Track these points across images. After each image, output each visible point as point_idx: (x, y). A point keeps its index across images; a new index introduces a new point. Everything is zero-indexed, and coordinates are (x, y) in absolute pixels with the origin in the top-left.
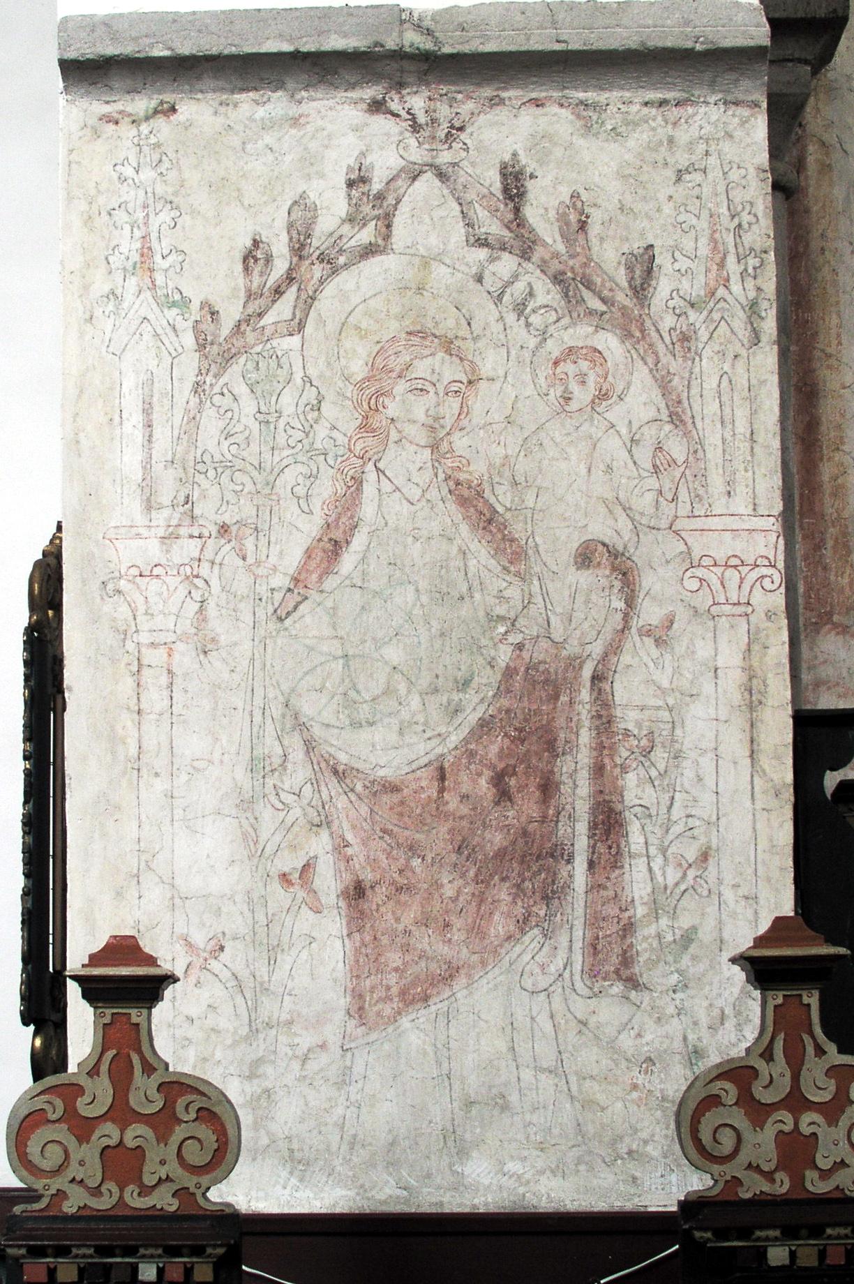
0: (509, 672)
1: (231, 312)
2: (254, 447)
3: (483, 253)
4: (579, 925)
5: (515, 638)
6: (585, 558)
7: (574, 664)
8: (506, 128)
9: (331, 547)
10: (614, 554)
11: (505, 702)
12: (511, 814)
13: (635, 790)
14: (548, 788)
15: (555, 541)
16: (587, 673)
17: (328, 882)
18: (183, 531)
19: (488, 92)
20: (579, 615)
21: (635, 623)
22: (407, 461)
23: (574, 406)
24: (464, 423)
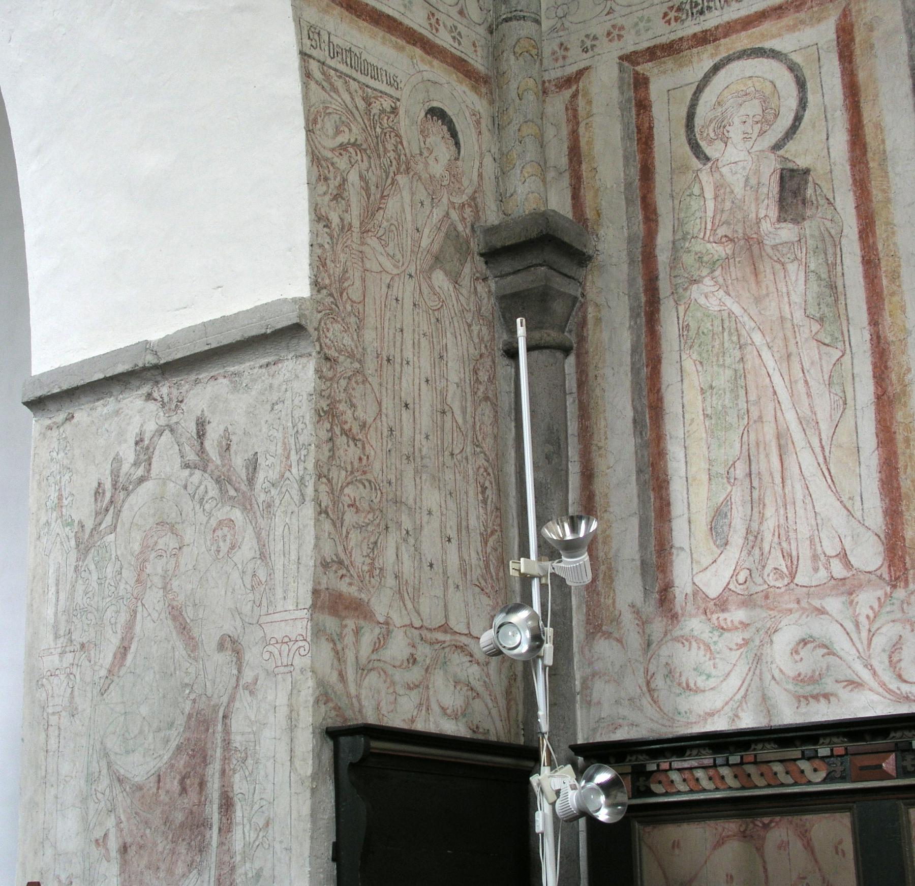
0: (190, 716)
1: (89, 524)
2: (96, 599)
3: (187, 472)
4: (213, 866)
5: (192, 697)
6: (221, 647)
7: (215, 709)
8: (204, 394)
9: (124, 651)
10: (234, 642)
11: (187, 735)
12: (185, 801)
13: (239, 785)
14: (202, 785)
15: (209, 636)
16: (221, 715)
17: (113, 844)
18: (67, 649)
19: (193, 377)
20: (218, 680)
21: (241, 683)
22: (154, 598)
23: (221, 554)
24: (177, 572)
